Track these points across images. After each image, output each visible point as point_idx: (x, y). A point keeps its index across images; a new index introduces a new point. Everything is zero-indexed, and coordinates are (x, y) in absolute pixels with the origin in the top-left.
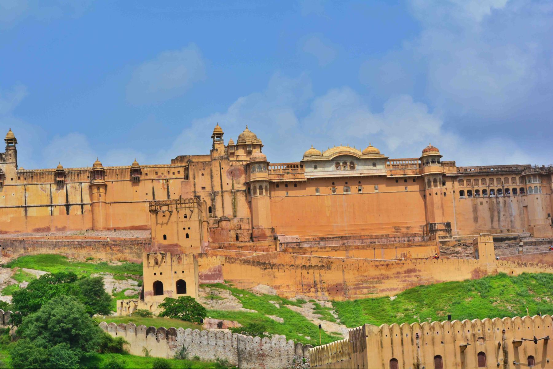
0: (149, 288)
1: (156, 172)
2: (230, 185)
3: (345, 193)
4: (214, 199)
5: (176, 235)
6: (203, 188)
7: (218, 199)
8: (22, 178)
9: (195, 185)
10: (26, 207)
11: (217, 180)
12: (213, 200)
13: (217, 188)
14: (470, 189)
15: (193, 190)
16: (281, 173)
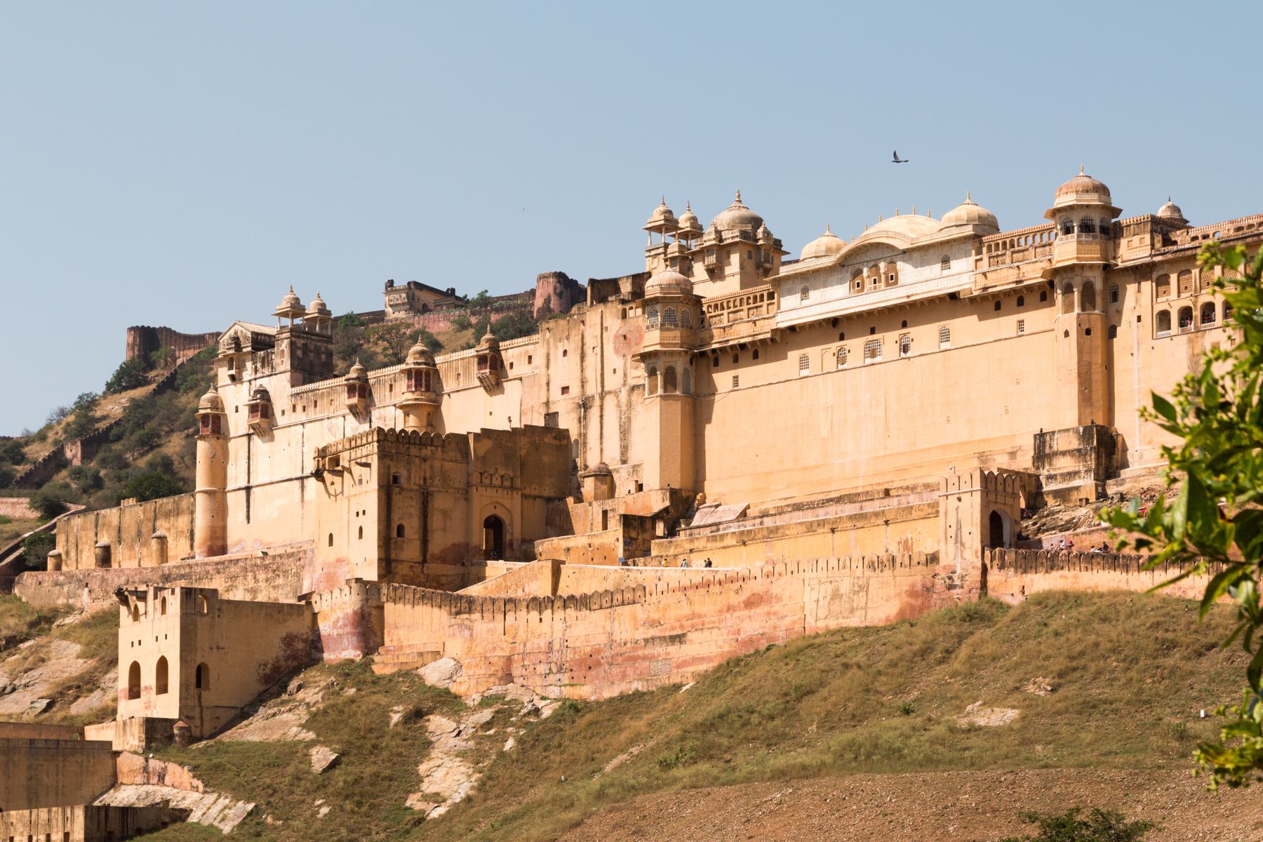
0: (123, 682)
1: (530, 357)
2: (620, 373)
3: (869, 361)
4: (585, 418)
5: (345, 533)
6: (565, 390)
7: (594, 413)
8: (299, 408)
9: (548, 384)
10: (302, 478)
11: (592, 360)
12: (583, 420)
13: (592, 389)
14: (1188, 303)
15: (545, 400)
16: (725, 323)
